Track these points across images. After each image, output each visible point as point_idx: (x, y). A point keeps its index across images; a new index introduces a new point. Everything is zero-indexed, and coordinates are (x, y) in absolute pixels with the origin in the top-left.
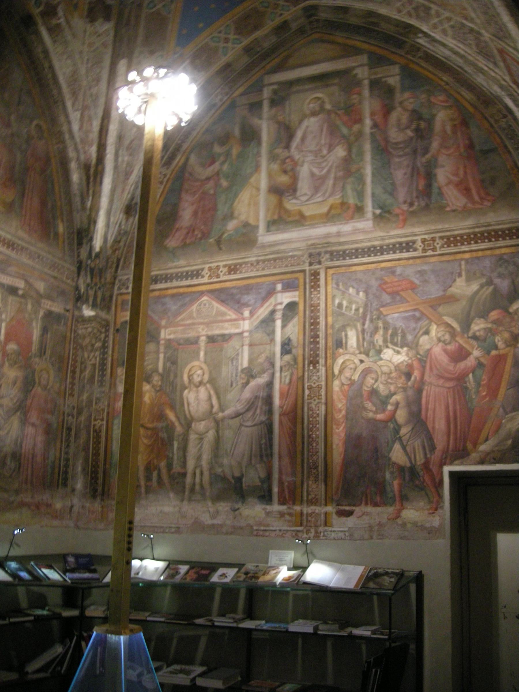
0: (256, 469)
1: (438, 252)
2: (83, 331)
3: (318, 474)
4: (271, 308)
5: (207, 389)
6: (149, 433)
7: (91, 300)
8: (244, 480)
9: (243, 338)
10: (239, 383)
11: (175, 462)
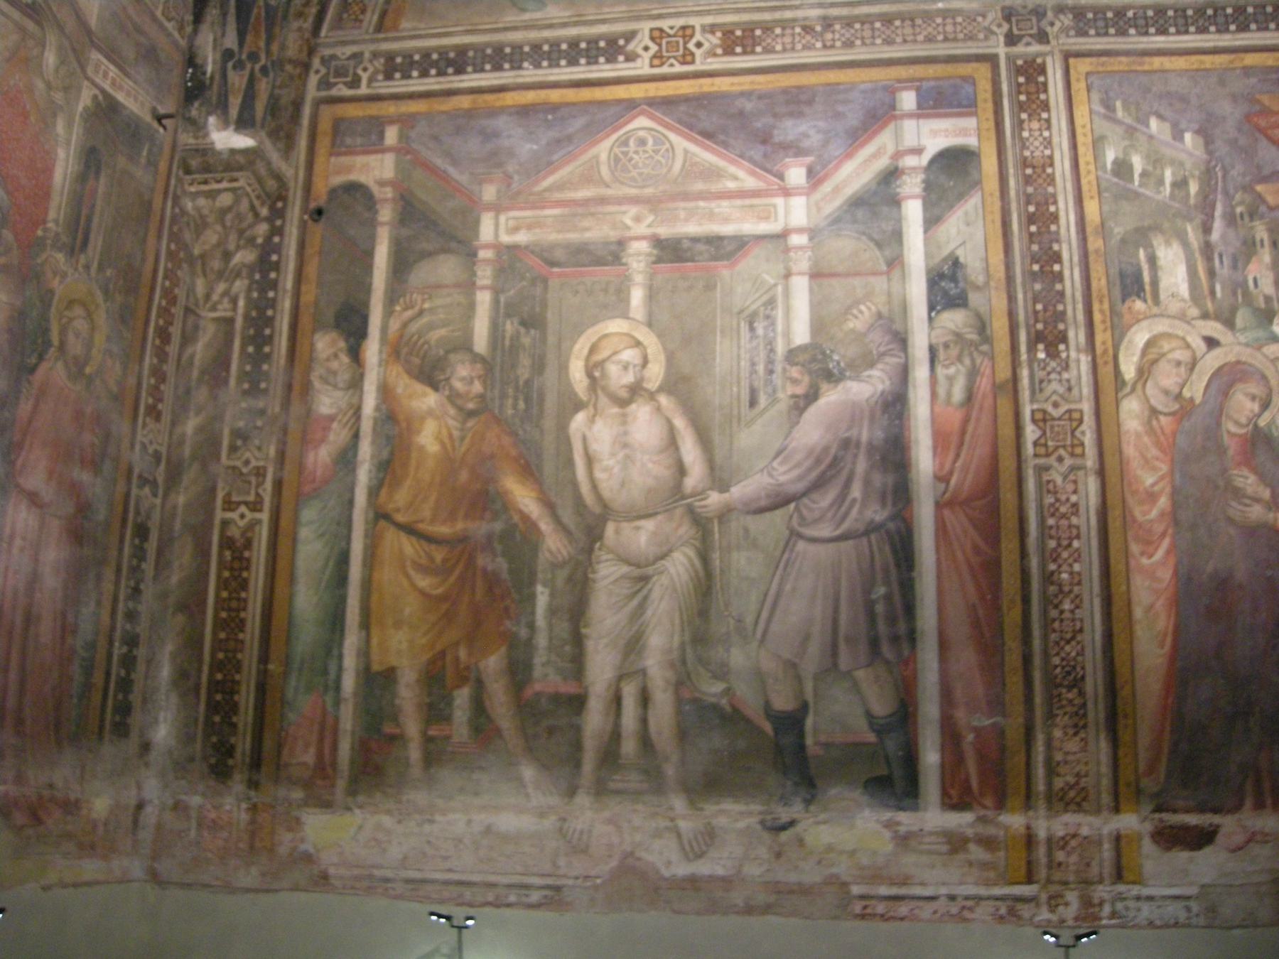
0: (856, 686)
2: (202, 202)
3: (1084, 705)
4: (883, 163)
5: (658, 409)
6: (439, 555)
7: (235, 103)
8: (809, 722)
9: (787, 250)
10: (781, 395)
11: (539, 659)
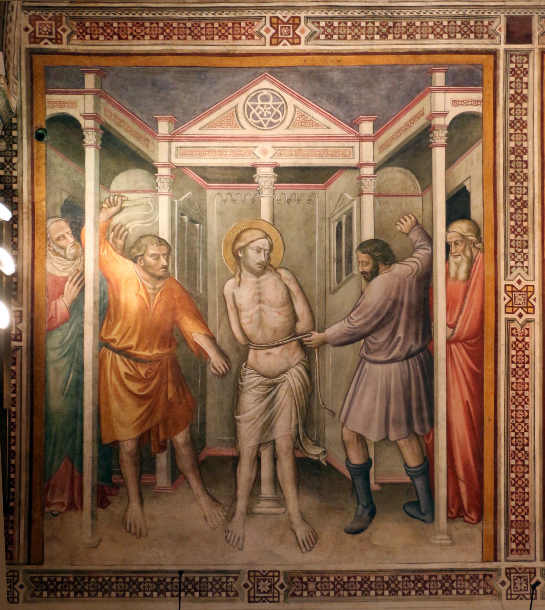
4: (422, 122)
8: (372, 470)
9: (360, 178)
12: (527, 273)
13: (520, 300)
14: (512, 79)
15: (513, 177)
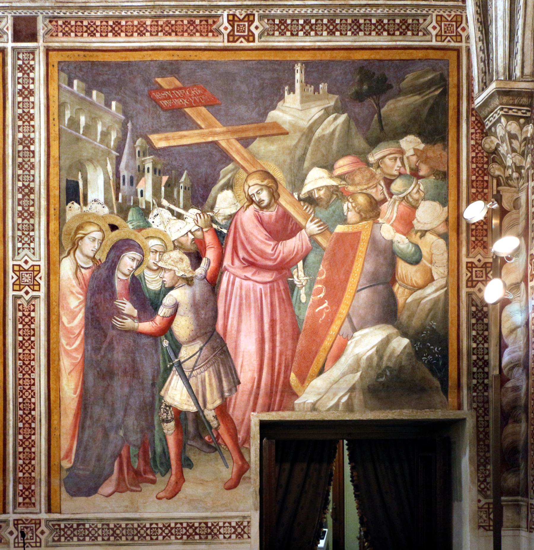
1: (257, 44)
12: (34, 254)
13: (27, 278)
14: (20, 75)
15: (21, 166)
